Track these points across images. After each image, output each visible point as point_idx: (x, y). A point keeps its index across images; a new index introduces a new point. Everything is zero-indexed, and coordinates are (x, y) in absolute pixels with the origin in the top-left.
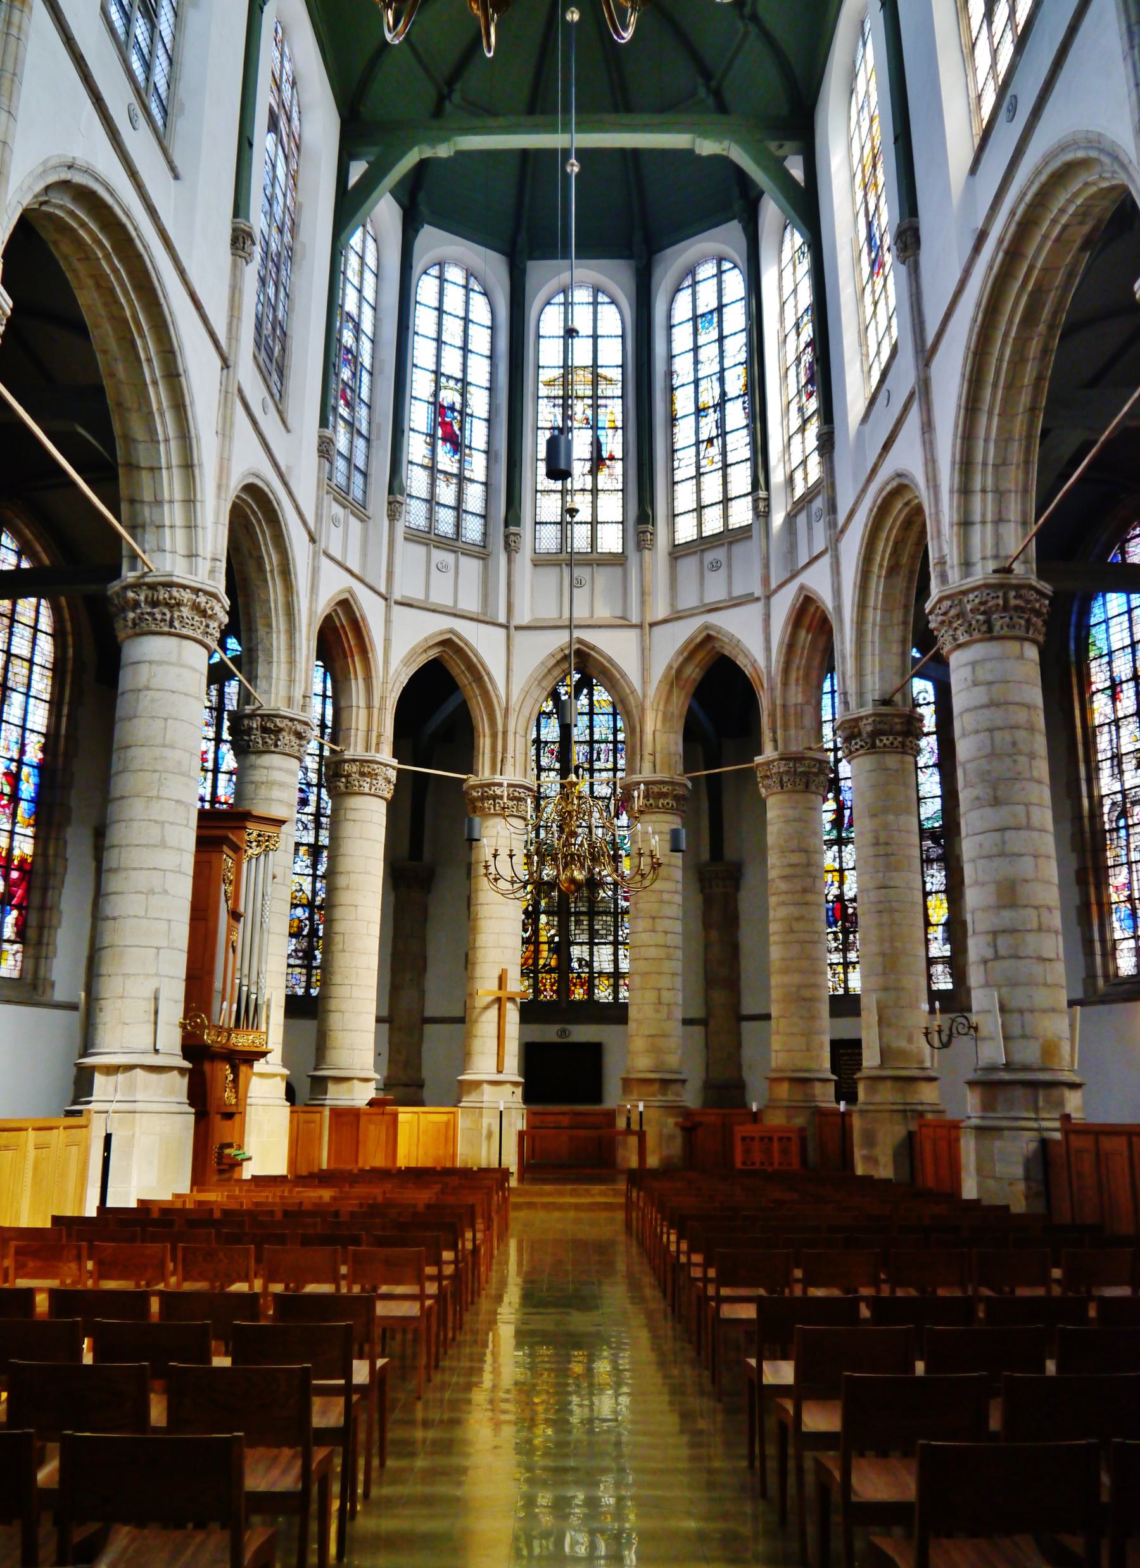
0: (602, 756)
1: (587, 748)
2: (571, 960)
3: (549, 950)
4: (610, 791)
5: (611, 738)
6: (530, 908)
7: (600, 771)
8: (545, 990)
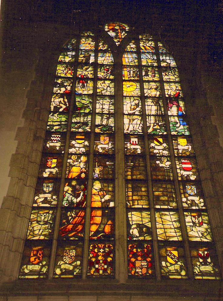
2: (129, 226)
3: (103, 216)
4: (158, 93)
5: (155, 64)
6: (83, 175)
7: (149, 82)
8: (98, 262)
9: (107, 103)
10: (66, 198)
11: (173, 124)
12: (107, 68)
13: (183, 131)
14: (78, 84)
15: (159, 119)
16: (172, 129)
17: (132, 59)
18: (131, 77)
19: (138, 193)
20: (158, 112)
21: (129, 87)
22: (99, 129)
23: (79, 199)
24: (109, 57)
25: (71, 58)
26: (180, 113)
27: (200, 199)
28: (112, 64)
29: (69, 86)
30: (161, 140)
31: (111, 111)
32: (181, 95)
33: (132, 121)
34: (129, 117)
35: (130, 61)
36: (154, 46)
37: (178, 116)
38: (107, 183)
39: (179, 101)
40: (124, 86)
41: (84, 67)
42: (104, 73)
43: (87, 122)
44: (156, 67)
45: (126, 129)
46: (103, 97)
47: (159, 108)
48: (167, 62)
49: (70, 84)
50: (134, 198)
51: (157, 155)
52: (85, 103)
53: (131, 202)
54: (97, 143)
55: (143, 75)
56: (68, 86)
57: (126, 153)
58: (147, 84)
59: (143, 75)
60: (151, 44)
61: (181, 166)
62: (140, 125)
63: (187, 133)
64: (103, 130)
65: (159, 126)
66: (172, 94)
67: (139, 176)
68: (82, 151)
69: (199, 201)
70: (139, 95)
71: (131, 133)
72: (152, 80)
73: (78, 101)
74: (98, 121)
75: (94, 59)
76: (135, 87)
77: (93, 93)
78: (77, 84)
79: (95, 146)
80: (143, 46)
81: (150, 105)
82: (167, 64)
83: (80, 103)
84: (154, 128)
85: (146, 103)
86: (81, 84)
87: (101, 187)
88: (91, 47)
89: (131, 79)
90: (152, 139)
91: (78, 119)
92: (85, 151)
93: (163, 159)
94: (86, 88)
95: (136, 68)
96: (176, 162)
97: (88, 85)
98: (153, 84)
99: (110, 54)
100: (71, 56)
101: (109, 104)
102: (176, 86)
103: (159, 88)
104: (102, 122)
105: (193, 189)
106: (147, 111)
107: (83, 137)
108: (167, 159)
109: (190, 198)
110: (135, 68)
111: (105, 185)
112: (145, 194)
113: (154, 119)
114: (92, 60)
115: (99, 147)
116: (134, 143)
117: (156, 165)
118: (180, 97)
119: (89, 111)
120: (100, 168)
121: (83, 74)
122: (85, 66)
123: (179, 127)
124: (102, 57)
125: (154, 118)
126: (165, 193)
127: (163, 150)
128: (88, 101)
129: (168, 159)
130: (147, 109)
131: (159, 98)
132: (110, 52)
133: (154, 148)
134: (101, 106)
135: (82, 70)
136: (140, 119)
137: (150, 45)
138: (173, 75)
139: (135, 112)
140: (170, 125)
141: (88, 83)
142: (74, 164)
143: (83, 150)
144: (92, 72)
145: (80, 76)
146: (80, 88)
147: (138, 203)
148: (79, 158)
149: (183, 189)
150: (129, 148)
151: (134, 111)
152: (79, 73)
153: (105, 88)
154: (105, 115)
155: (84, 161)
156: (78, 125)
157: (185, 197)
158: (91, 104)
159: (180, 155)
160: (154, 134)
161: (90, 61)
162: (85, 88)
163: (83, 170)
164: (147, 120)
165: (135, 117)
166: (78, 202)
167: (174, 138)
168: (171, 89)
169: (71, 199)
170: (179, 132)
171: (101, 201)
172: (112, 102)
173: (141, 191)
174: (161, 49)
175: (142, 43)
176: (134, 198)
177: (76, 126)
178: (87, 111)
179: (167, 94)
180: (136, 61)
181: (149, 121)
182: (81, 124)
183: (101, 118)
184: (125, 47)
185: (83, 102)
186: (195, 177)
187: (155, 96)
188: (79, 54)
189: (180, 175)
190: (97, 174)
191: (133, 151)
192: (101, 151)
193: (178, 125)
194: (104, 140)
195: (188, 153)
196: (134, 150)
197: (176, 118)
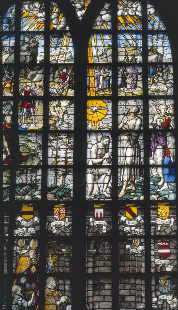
0: (129, 81)
1: (110, 73)
4: (138, 122)
5: (140, 59)
6: (34, 269)
7: (126, 98)
9: (63, 147)
10: (15, 300)
11: (154, 182)
12: (63, 73)
13: (167, 192)
14: (21, 109)
15: (136, 174)
16: (152, 190)
17: (103, 47)
18: (99, 90)
19: (100, 292)
20: (135, 160)
21: (96, 111)
22: (52, 195)
23: (30, 302)
24: (66, 46)
25: (8, 55)
26: (167, 160)
27: (173, 298)
28: (72, 62)
29: (9, 115)
30: (134, 210)
31: (69, 160)
32: (171, 124)
33: (97, 177)
34: (93, 170)
35: (99, 55)
36: (140, 15)
37: (163, 166)
38: (64, 279)
39: (168, 137)
40: (89, 111)
41: (29, 73)
42: (59, 83)
43: (36, 183)
44: (139, 65)
45: (88, 194)
46: (57, 133)
47: (137, 153)
48: (158, 53)
49: (10, 111)
50: (96, 299)
51: (128, 235)
52: (32, 148)
53: (91, 305)
54: (50, 218)
55: (119, 84)
56: (6, 116)
57: (88, 234)
58: (123, 103)
59: (119, 84)
60: (136, 10)
61: (157, 252)
62: (107, 185)
63: (172, 197)
64: (57, 197)
65: (135, 185)
66: (159, 124)
67: (102, 268)
68: (31, 232)
69: (171, 300)
70: (109, 127)
71: (95, 200)
72: (131, 95)
73: (23, 145)
74: (51, 182)
75: (43, 54)
76: (105, 112)
77: (42, 127)
78: (19, 111)
79: (47, 223)
80: (123, 16)
81: (124, 148)
82: (157, 58)
83: (25, 148)
84: (127, 188)
85: (119, 143)
86: (25, 110)
87: (55, 286)
88: (38, 25)
89: (100, 94)
90: (122, 209)
91: (23, 177)
92: (34, 233)
93: (135, 241)
94: (33, 117)
95: (109, 69)
96: (152, 245)
97: (35, 112)
98: (132, 103)
99: (68, 39)
100: (8, 48)
101: (66, 148)
102: (167, 105)
103: (141, 111)
104: (57, 181)
105: (167, 284)
106: (119, 158)
107: (31, 209)
108: (140, 241)
109: (161, 297)
110: (106, 70)
111: (61, 282)
112: (109, 294)
113: (129, 174)
114: (40, 58)
115: (52, 224)
116: (99, 217)
117: (124, 252)
118: (170, 128)
119: (37, 162)
120: (54, 258)
121: (28, 89)
122: (31, 71)
123: (162, 186)
124: (56, 47)
125: (129, 171)
126: (133, 291)
127: (137, 226)
128: (36, 143)
129: (142, 241)
130: (119, 155)
131: (139, 132)
132: (69, 34)
133: (124, 223)
134: (55, 153)
135: (25, 81)
136: (109, 174)
137: (134, 14)
138: (164, 82)
139: (102, 162)
140: (151, 183)
141: (35, 108)
142: (22, 253)
143: (31, 230)
144: (41, 83)
145: (23, 94)
146: (25, 118)
147: (99, 306)
148: (27, 243)
149: (155, 286)
150: (92, 224)
151: (100, 160)
152: (22, 86)
153: (61, 117)
154: (61, 169)
155: (34, 248)
156: (24, 188)
157: (157, 296)
158: (40, 150)
159: (158, 233)
160: (127, 201)
161: (38, 57)
162: (31, 118)
163: (33, 261)
164: (119, 174)
165: (102, 170)
166: (29, 306)
167: (152, 206)
168: (159, 113)
169: (21, 302)
170: (160, 196)
171: (56, 305)
172: (70, 143)
173: (104, 289)
174: (152, 22)
175: (121, 7)
176: (96, 299)
177: (22, 190)
178: (36, 162)
179: (152, 124)
180: (109, 52)
181: (122, 176)
182: (28, 187)
183: (54, 174)
184: (93, 22)
185: (30, 145)
186: (172, 267)
187: (133, 126)
188: (21, 44)
189: (153, 265)
190: (50, 267)
191: (97, 230)
192: (55, 231)
193: (160, 183)
194: (60, 214)
195: (168, 231)
196: (98, 228)
197: (160, 170)
